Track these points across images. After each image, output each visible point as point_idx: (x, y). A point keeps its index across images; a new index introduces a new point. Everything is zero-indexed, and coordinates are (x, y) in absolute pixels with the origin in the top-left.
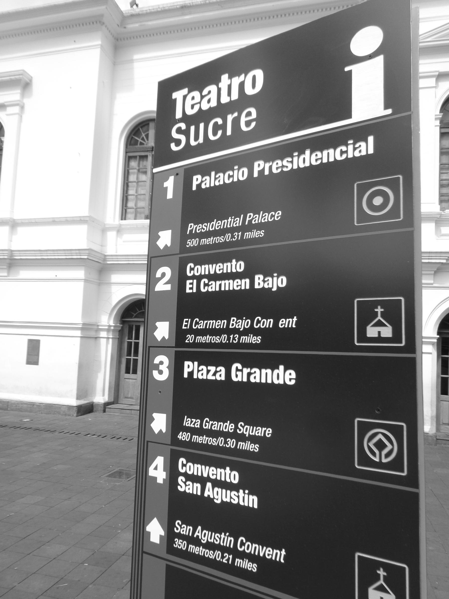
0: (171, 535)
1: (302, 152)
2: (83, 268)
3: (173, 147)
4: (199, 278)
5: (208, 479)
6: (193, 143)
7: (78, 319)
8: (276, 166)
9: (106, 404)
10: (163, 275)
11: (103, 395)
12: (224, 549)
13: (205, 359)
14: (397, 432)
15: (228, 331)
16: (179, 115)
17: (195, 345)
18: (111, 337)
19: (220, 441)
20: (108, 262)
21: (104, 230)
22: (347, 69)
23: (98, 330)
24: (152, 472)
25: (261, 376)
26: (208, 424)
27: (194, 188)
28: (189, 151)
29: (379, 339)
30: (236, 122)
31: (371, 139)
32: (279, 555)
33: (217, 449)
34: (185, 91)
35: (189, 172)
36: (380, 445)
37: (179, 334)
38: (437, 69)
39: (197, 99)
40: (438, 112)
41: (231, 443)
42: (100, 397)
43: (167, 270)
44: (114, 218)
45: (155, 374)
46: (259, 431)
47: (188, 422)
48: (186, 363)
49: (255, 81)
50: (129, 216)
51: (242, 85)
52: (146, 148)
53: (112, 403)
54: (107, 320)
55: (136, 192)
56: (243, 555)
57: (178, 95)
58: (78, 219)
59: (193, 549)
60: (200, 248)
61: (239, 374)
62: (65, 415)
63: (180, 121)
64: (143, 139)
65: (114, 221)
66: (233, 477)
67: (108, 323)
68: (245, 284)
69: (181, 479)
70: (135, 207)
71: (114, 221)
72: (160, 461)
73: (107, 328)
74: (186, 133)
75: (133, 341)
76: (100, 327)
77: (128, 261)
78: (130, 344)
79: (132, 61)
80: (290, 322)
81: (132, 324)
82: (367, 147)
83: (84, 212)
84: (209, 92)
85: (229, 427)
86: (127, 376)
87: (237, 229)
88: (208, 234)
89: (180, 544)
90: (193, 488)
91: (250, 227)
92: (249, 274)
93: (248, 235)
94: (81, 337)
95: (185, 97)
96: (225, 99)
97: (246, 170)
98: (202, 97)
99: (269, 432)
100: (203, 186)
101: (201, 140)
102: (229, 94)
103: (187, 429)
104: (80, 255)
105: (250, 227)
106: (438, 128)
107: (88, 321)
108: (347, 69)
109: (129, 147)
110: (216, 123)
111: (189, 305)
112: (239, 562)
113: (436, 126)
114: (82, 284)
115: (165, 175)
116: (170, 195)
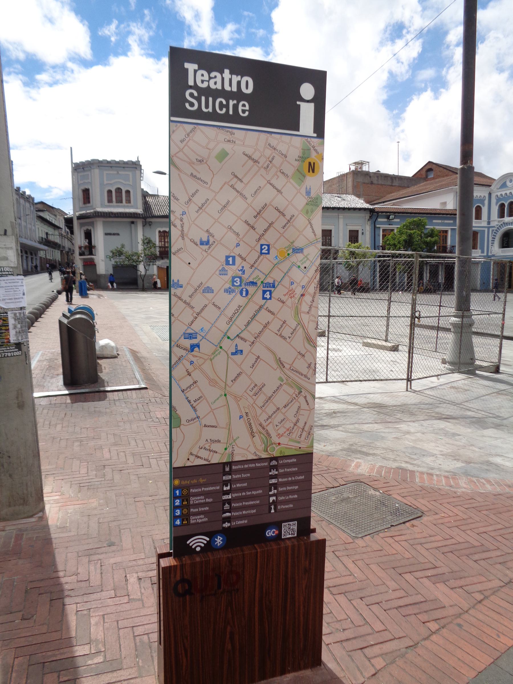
3: (187, 105)
6: (204, 109)
16: (191, 83)
22: (298, 103)
30: (236, 107)
34: (196, 67)
39: (206, 77)
51: (239, 83)
63: (191, 87)
84: (215, 77)
98: (210, 78)
101: (210, 109)
102: (230, 85)
108: (298, 103)
110: (221, 103)
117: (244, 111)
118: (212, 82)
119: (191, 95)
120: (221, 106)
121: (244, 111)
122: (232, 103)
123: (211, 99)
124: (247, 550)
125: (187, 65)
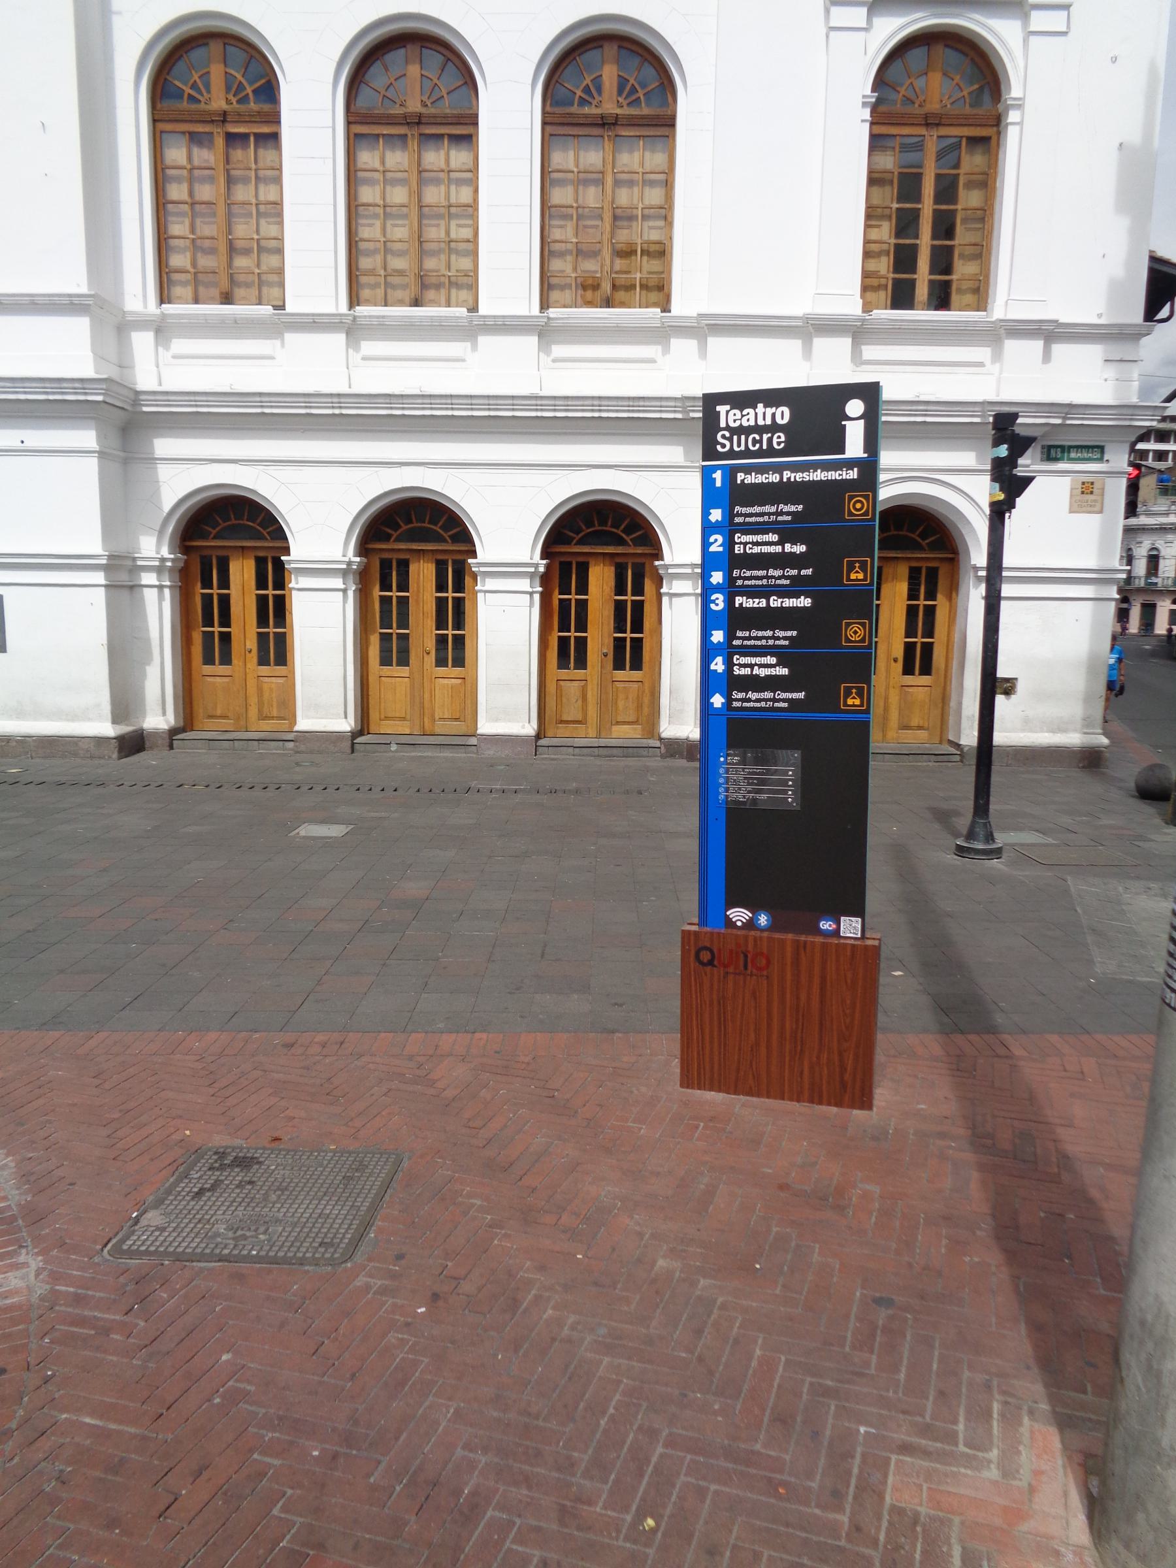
0: (729, 700)
1: (815, 471)
3: (719, 448)
4: (745, 544)
6: (736, 448)
7: (93, 544)
8: (799, 477)
9: (173, 732)
10: (716, 540)
11: (164, 714)
13: (751, 593)
14: (863, 625)
15: (767, 577)
16: (723, 424)
18: (168, 583)
19: (764, 642)
20: (145, 409)
21: (124, 326)
23: (135, 570)
24: (713, 667)
25: (789, 603)
26: (754, 633)
29: (857, 580)
30: (770, 440)
32: (801, 695)
33: (762, 647)
34: (728, 407)
35: (734, 470)
36: (855, 633)
37: (730, 580)
39: (739, 416)
40: (868, 92)
41: (771, 642)
42: (158, 717)
43: (720, 538)
44: (145, 296)
45: (713, 606)
46: (789, 634)
47: (739, 634)
49: (783, 415)
50: (177, 291)
51: (774, 415)
52: (209, 113)
53: (183, 730)
54: (154, 547)
56: (779, 701)
57: (722, 409)
58: (66, 301)
59: (746, 704)
60: (744, 524)
61: (775, 602)
62: (92, 757)
63: (724, 429)
64: (194, 86)
65: (145, 306)
66: (773, 660)
67: (158, 553)
68: (778, 549)
70: (192, 270)
71: (145, 306)
72: (719, 659)
73: (157, 563)
74: (731, 440)
76: (139, 563)
77: (196, 406)
80: (809, 572)
81: (206, 553)
82: (853, 474)
83: (76, 282)
85: (769, 633)
86: (208, 669)
87: (773, 514)
88: (751, 515)
89: (736, 704)
90: (747, 671)
91: (782, 513)
92: (781, 542)
93: (780, 518)
94: (106, 586)
95: (728, 412)
96: (761, 422)
99: (795, 633)
101: (743, 448)
103: (739, 638)
104: (86, 394)
105: (782, 513)
106: (868, 125)
109: (159, 106)
111: (734, 561)
112: (776, 705)
113: (863, 121)
114: (93, 463)
115: (714, 469)
116: (718, 484)
118: (745, 419)
119: (723, 437)
120: (755, 442)
121: (779, 443)
122: (765, 437)
123: (743, 437)
125: (718, 408)
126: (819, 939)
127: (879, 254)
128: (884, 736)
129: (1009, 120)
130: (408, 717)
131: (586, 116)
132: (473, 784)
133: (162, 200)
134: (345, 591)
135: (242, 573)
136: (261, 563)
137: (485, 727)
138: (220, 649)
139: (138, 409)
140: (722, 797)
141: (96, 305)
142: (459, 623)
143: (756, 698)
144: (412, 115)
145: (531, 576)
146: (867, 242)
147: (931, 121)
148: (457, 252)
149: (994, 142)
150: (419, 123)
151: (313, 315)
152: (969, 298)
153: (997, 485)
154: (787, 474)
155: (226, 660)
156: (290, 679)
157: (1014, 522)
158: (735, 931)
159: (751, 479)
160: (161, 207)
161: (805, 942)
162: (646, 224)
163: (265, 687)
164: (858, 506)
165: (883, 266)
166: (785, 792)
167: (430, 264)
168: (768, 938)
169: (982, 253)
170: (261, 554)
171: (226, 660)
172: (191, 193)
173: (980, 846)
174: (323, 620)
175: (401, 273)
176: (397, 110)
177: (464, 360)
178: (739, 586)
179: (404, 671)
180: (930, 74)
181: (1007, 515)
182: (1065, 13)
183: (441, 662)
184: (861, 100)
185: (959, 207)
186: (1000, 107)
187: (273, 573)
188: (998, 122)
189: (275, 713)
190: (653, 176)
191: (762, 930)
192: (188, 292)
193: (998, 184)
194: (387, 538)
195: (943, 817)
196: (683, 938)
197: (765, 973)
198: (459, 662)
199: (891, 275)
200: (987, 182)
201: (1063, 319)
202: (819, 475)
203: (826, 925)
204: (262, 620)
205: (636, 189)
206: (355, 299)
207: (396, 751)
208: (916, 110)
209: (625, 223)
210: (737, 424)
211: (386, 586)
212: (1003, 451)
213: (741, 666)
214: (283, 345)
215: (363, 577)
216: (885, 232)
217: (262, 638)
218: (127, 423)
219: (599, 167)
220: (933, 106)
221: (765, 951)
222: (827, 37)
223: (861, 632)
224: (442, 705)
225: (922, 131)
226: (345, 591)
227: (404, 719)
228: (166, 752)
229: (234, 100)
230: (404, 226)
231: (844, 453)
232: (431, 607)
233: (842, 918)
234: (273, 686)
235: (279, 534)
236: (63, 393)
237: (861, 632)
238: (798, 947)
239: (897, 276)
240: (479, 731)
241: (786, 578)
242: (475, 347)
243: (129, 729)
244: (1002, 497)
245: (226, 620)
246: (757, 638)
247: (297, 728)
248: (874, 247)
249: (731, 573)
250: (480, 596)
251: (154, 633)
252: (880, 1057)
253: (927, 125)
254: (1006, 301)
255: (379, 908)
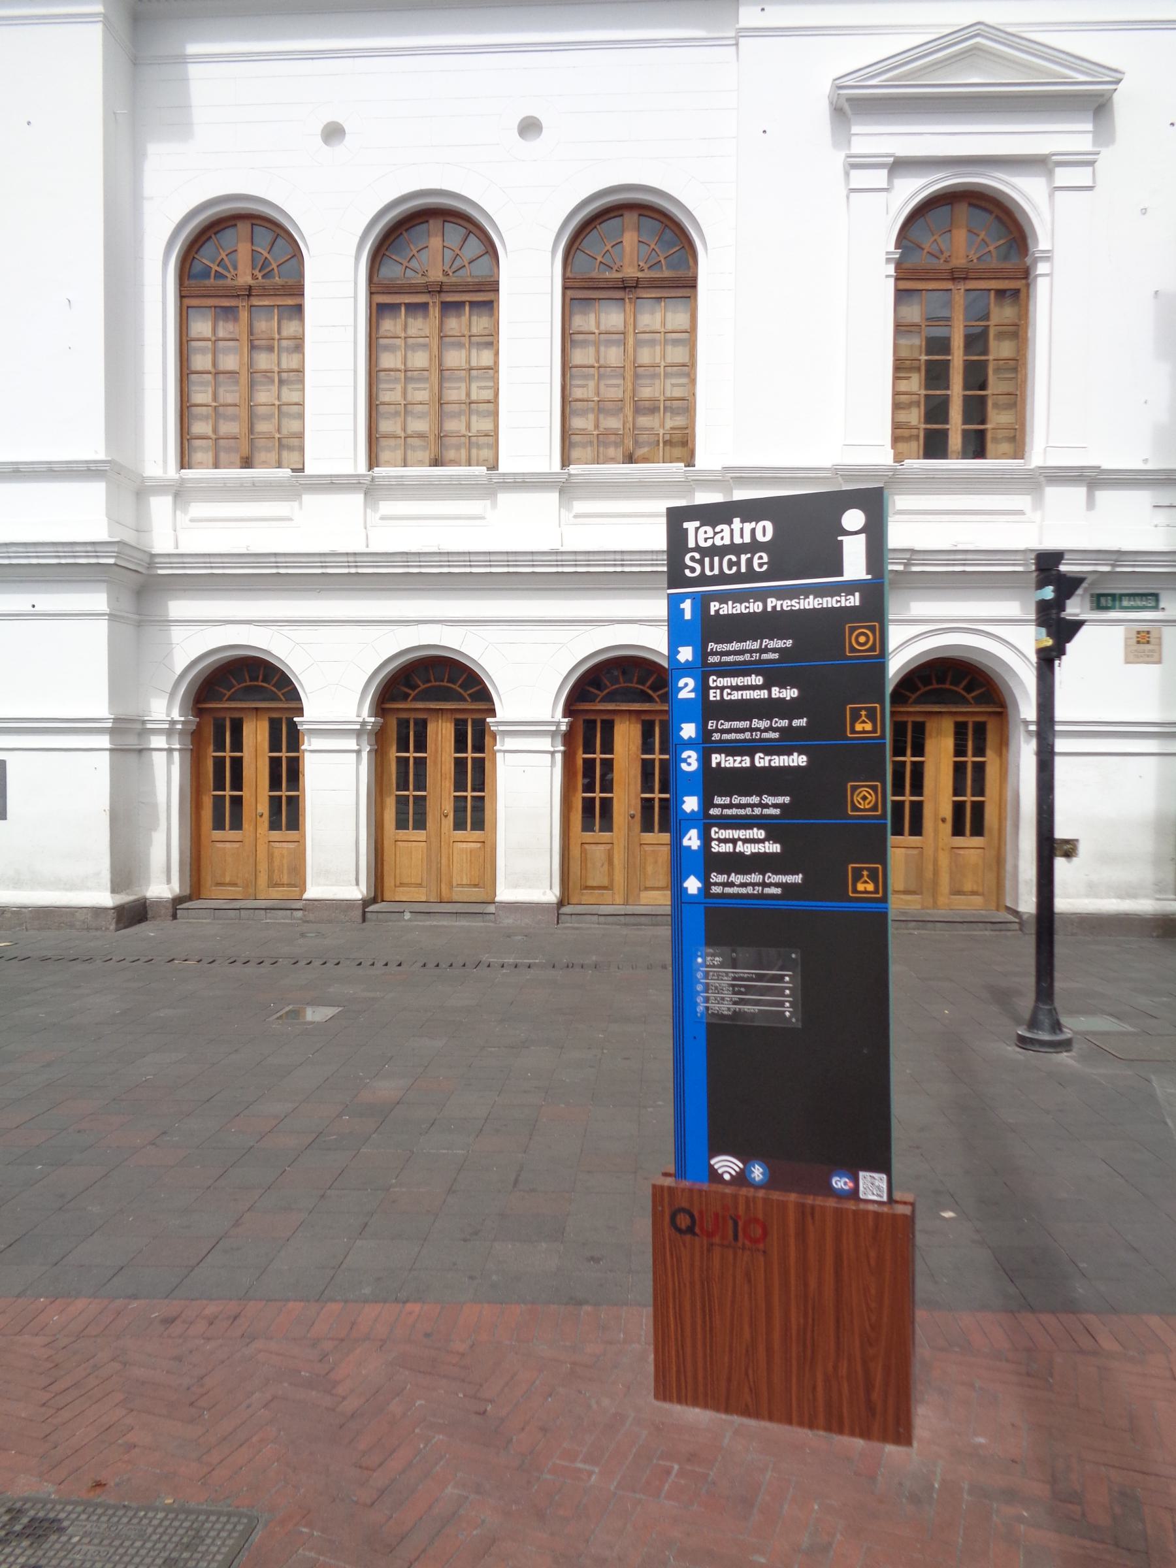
0: (707, 884)
1: (807, 597)
2: (104, 585)
3: (687, 572)
4: (722, 689)
5: (739, 839)
6: (708, 573)
7: (99, 708)
8: (787, 605)
9: (177, 901)
10: (686, 685)
11: (169, 881)
12: (753, 885)
13: (732, 749)
14: (874, 788)
15: (751, 730)
16: (691, 544)
17: (721, 741)
18: (178, 746)
19: (748, 811)
20: (160, 572)
21: (142, 491)
22: (840, 538)
23: (145, 732)
24: (686, 842)
25: (779, 761)
26: (736, 800)
27: (712, 613)
28: (703, 580)
30: (749, 562)
31: (857, 594)
32: (798, 878)
34: (697, 524)
36: (864, 798)
38: (890, 151)
40: (892, 248)
41: (757, 811)
42: (161, 887)
44: (165, 462)
45: (684, 766)
46: (780, 800)
47: (718, 800)
48: (714, 756)
49: (765, 531)
50: (198, 456)
51: (753, 531)
52: (233, 288)
53: (189, 898)
54: (165, 709)
55: (215, 398)
56: (770, 885)
57: (690, 526)
58: (83, 467)
59: (728, 890)
60: (720, 664)
61: (761, 760)
62: (88, 929)
63: (693, 550)
65: (165, 472)
66: (761, 834)
67: (168, 716)
68: (764, 694)
69: (714, 844)
70: (214, 437)
71: (165, 472)
72: (693, 833)
73: (167, 726)
74: (701, 562)
75: (228, 754)
76: (149, 726)
78: (219, 763)
79: (183, 59)
80: (802, 722)
81: (221, 715)
82: (854, 600)
83: (94, 449)
85: (755, 799)
86: (218, 835)
88: (728, 653)
89: (716, 890)
90: (729, 848)
91: (766, 650)
92: (767, 686)
93: (765, 656)
94: (111, 750)
95: (697, 529)
96: (738, 540)
97: (760, 604)
98: (715, 533)
99: (787, 799)
100: (721, 612)
101: (716, 571)
102: (742, 537)
105: (766, 650)
106: (892, 280)
107: (124, 712)
108: (840, 538)
109: (186, 283)
110: (730, 560)
112: (767, 891)
113: (887, 276)
114: (103, 625)
116: (688, 616)
117: (761, 565)
118: (718, 536)
119: (693, 559)
120: (731, 564)
121: (761, 565)
123: (716, 559)
124: (793, 1197)
125: (686, 525)
126: (831, 1203)
127: (909, 405)
128: (935, 902)
129: (1038, 272)
130: (424, 884)
131: (607, 280)
132: (485, 958)
133: (185, 371)
134: (358, 752)
135: (256, 734)
136: (275, 727)
137: (505, 893)
138: (230, 814)
139: (153, 572)
140: (700, 1009)
141: (113, 472)
142: (480, 785)
143: (741, 883)
144: (433, 283)
145: (553, 734)
146: (896, 394)
147: (956, 276)
148: (478, 413)
149: (1023, 295)
150: (439, 292)
151: (331, 476)
152: (1005, 447)
153: (1043, 630)
154: (771, 602)
155: (237, 824)
156: (301, 843)
157: (1064, 670)
158: (720, 1188)
159: (728, 609)
160: (185, 378)
161: (813, 1207)
162: (669, 382)
163: (276, 853)
164: (862, 639)
165: (914, 417)
166: (782, 1004)
167: (451, 425)
168: (765, 1200)
169: (1017, 401)
170: (275, 715)
171: (237, 824)
172: (214, 364)
173: (1045, 1036)
174: (337, 784)
175: (421, 436)
176: (420, 280)
177: (482, 518)
178: (716, 742)
179: (421, 835)
180: (954, 232)
181: (1057, 662)
182: (1090, 169)
183: (459, 825)
184: (884, 257)
185: (991, 357)
186: (1028, 260)
187: (287, 736)
188: (1026, 275)
189: (285, 880)
190: (674, 336)
191: (757, 1187)
192: (209, 457)
193: (1029, 334)
194: (405, 697)
195: (1002, 997)
196: (654, 1195)
197: (761, 1246)
198: (479, 824)
199: (923, 426)
200: (1019, 332)
201: (1106, 465)
202: (811, 603)
203: (840, 1183)
204: (275, 783)
205: (658, 349)
206: (374, 460)
207: (409, 920)
208: (939, 264)
209: (648, 382)
210: (709, 543)
211: (403, 746)
212: (1048, 593)
213: (720, 841)
214: (301, 508)
215: (379, 737)
216: (914, 384)
217: (275, 803)
218: (140, 585)
219: (621, 328)
220: (959, 261)
221: (760, 1216)
222: (848, 198)
223: (871, 798)
224: (461, 872)
225: (949, 285)
226: (358, 752)
227: (420, 885)
228: (169, 924)
229: (260, 276)
230: (425, 389)
231: (842, 575)
232: (449, 768)
233: (861, 1174)
234: (285, 852)
235: (293, 695)
236: (75, 557)
237: (871, 798)
238: (803, 1211)
239: (929, 426)
240: (498, 899)
241: (774, 730)
242: (494, 505)
243: (131, 898)
244: (1049, 642)
245: (237, 784)
246: (740, 806)
247: (305, 896)
248: (903, 398)
249: (705, 724)
250: (499, 756)
251: (161, 798)
252: (923, 1350)
253: (953, 279)
254: (1042, 450)
255: (339, 1116)
